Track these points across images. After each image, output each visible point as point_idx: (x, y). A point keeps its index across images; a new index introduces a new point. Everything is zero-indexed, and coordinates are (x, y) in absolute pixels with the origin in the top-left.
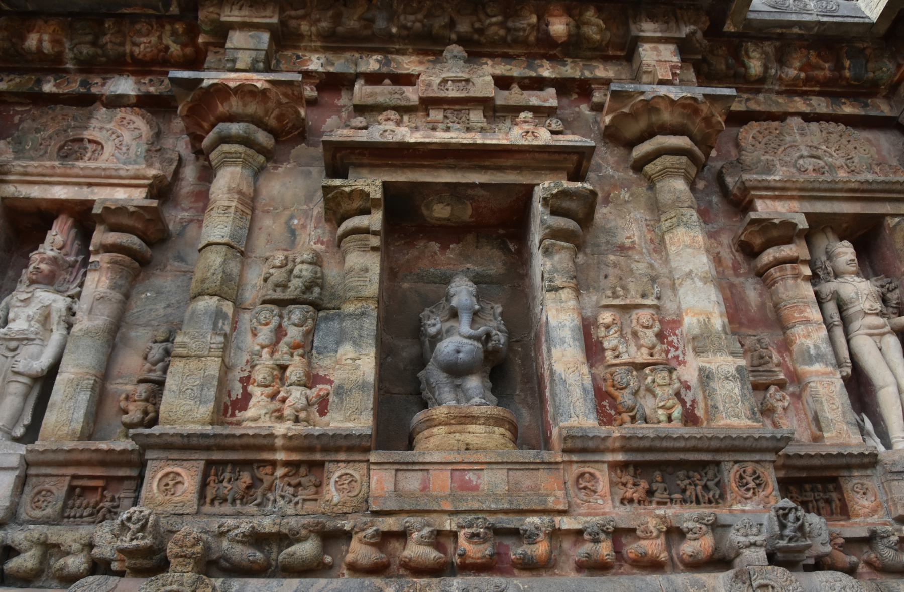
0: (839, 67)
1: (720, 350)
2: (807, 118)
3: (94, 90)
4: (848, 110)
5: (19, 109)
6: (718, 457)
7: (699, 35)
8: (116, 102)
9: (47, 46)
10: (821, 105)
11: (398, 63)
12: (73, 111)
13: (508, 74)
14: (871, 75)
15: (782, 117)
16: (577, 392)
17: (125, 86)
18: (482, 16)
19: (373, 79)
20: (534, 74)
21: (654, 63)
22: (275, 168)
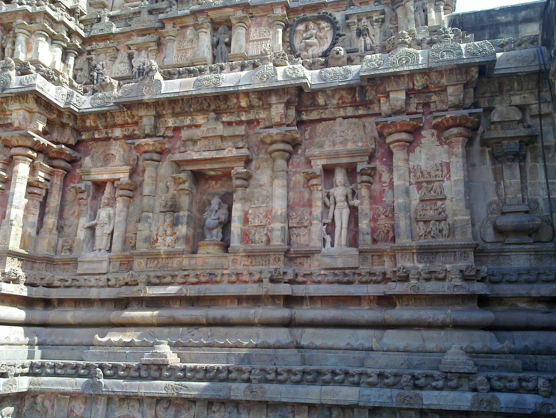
0: (354, 96)
1: (277, 222)
2: (344, 118)
3: (110, 136)
4: (361, 112)
5: (90, 143)
6: (269, 254)
7: (293, 98)
8: (116, 139)
9: (93, 124)
10: (350, 111)
11: (196, 120)
12: (105, 143)
13: (231, 120)
14: (367, 99)
15: (334, 119)
16: (236, 236)
17: (118, 132)
18: (219, 102)
19: (189, 127)
20: (239, 119)
21: (275, 114)
22: (162, 164)
